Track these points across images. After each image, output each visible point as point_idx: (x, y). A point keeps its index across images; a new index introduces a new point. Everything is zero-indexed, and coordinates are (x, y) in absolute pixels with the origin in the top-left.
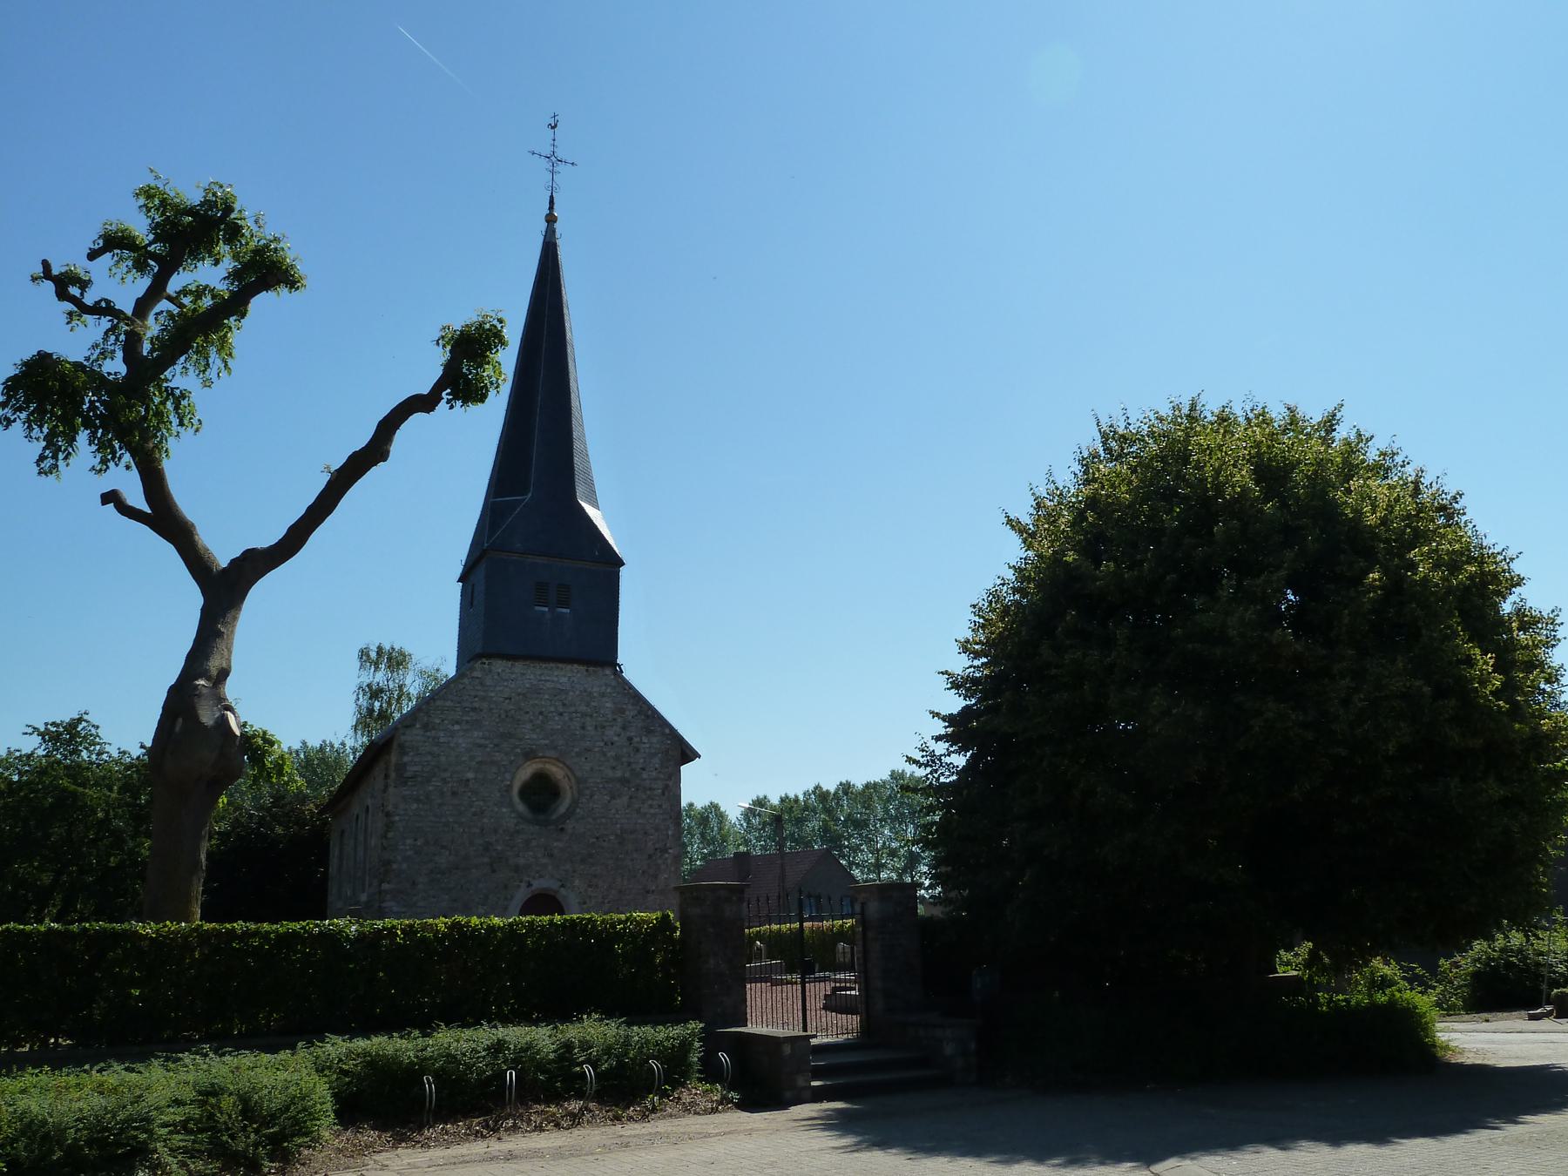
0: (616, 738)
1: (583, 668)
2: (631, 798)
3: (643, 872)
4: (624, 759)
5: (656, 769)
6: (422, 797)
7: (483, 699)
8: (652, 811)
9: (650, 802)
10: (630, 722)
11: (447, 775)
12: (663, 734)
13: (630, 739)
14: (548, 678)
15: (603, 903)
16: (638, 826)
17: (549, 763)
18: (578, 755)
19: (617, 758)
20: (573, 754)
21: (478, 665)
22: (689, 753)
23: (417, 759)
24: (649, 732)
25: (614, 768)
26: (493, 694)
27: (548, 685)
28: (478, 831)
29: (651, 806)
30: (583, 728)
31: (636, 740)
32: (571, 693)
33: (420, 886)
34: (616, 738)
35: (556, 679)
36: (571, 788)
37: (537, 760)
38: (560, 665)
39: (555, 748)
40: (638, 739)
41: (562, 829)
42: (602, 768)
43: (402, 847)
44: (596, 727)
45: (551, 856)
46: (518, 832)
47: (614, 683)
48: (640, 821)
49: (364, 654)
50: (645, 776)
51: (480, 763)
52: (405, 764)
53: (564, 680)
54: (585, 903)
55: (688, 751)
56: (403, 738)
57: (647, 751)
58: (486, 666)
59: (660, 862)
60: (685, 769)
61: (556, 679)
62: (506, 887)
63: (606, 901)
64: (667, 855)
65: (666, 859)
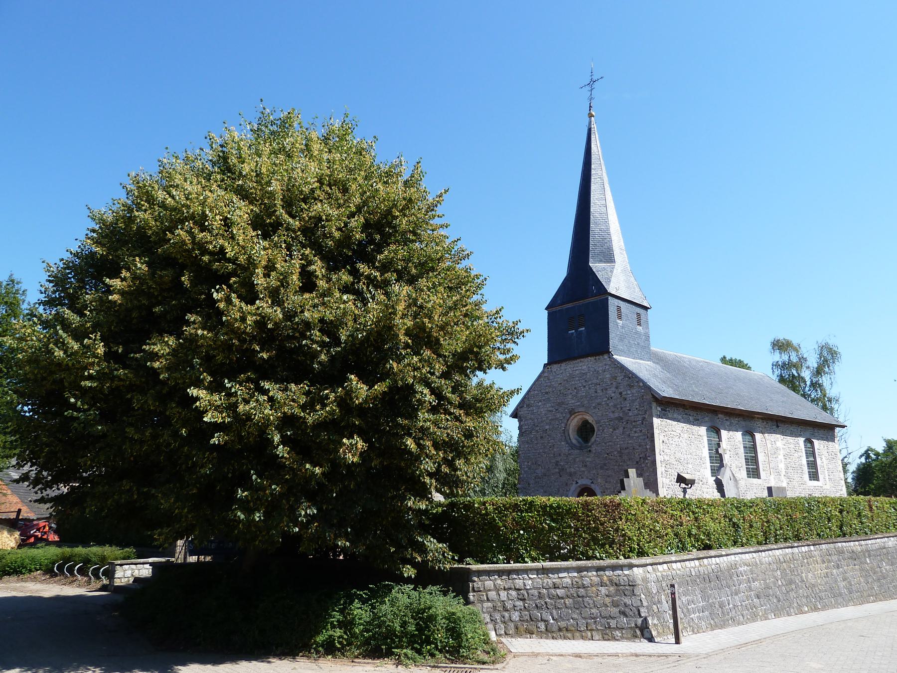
0: (613, 395)
1: (593, 358)
2: (624, 428)
4: (618, 406)
7: (550, 387)
8: (636, 435)
9: (634, 429)
11: (538, 428)
13: (621, 393)
18: (595, 408)
19: (615, 406)
20: (592, 408)
23: (526, 423)
24: (631, 387)
25: (613, 412)
27: (577, 372)
29: (635, 432)
32: (588, 374)
34: (613, 395)
38: (582, 360)
40: (625, 393)
41: (590, 451)
42: (607, 413)
44: (602, 391)
45: (586, 466)
46: (569, 454)
47: (609, 363)
48: (629, 442)
53: (584, 367)
56: (520, 413)
57: (631, 398)
58: (549, 369)
62: (567, 484)
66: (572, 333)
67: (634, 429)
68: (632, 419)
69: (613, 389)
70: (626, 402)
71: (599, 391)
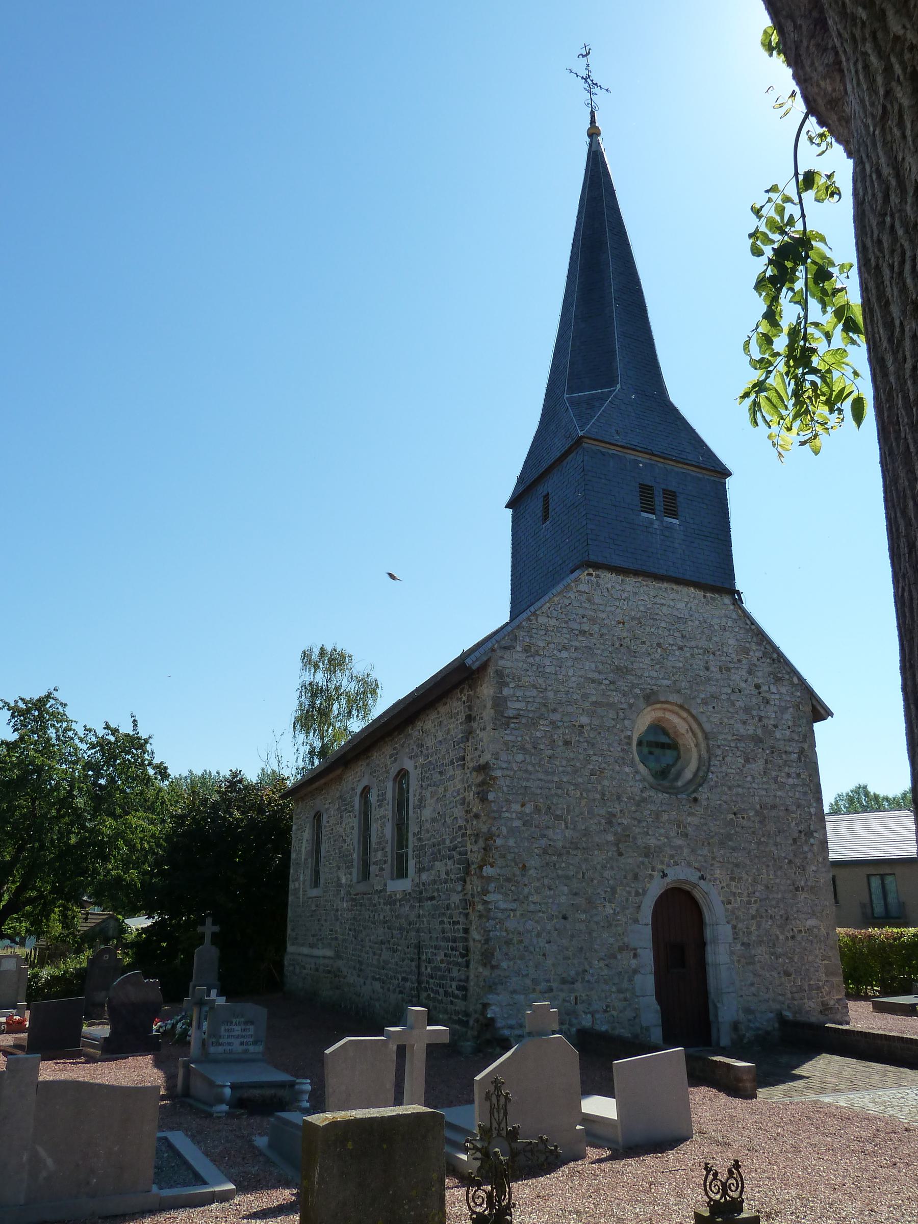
0: (743, 685)
1: (700, 594)
2: (766, 761)
3: (790, 862)
4: (754, 713)
5: (789, 728)
6: (527, 746)
7: (593, 620)
8: (791, 781)
9: (786, 769)
10: (755, 666)
11: (556, 717)
12: (792, 684)
13: (758, 687)
14: (663, 602)
15: (749, 903)
16: (778, 800)
17: (670, 711)
18: (705, 702)
20: (699, 701)
21: (584, 576)
22: (822, 712)
23: (519, 693)
24: (778, 680)
25: (744, 723)
26: (603, 615)
28: (598, 796)
29: (788, 775)
30: (707, 669)
31: (764, 688)
32: (690, 623)
33: (532, 872)
34: (743, 685)
35: (672, 603)
36: (697, 745)
37: (658, 706)
38: (675, 587)
39: (679, 692)
41: (695, 800)
42: (732, 722)
43: (507, 815)
47: (734, 616)
48: (779, 793)
49: (306, 656)
51: (594, 704)
52: (505, 699)
54: (729, 903)
55: (819, 708)
56: (501, 663)
57: (777, 702)
58: (593, 578)
59: (806, 849)
60: (818, 727)
61: (672, 603)
62: (636, 877)
63: (753, 900)
64: (812, 840)
65: (812, 845)
66: (651, 522)
68: (781, 745)
69: (744, 673)
70: (768, 706)
71: (712, 668)
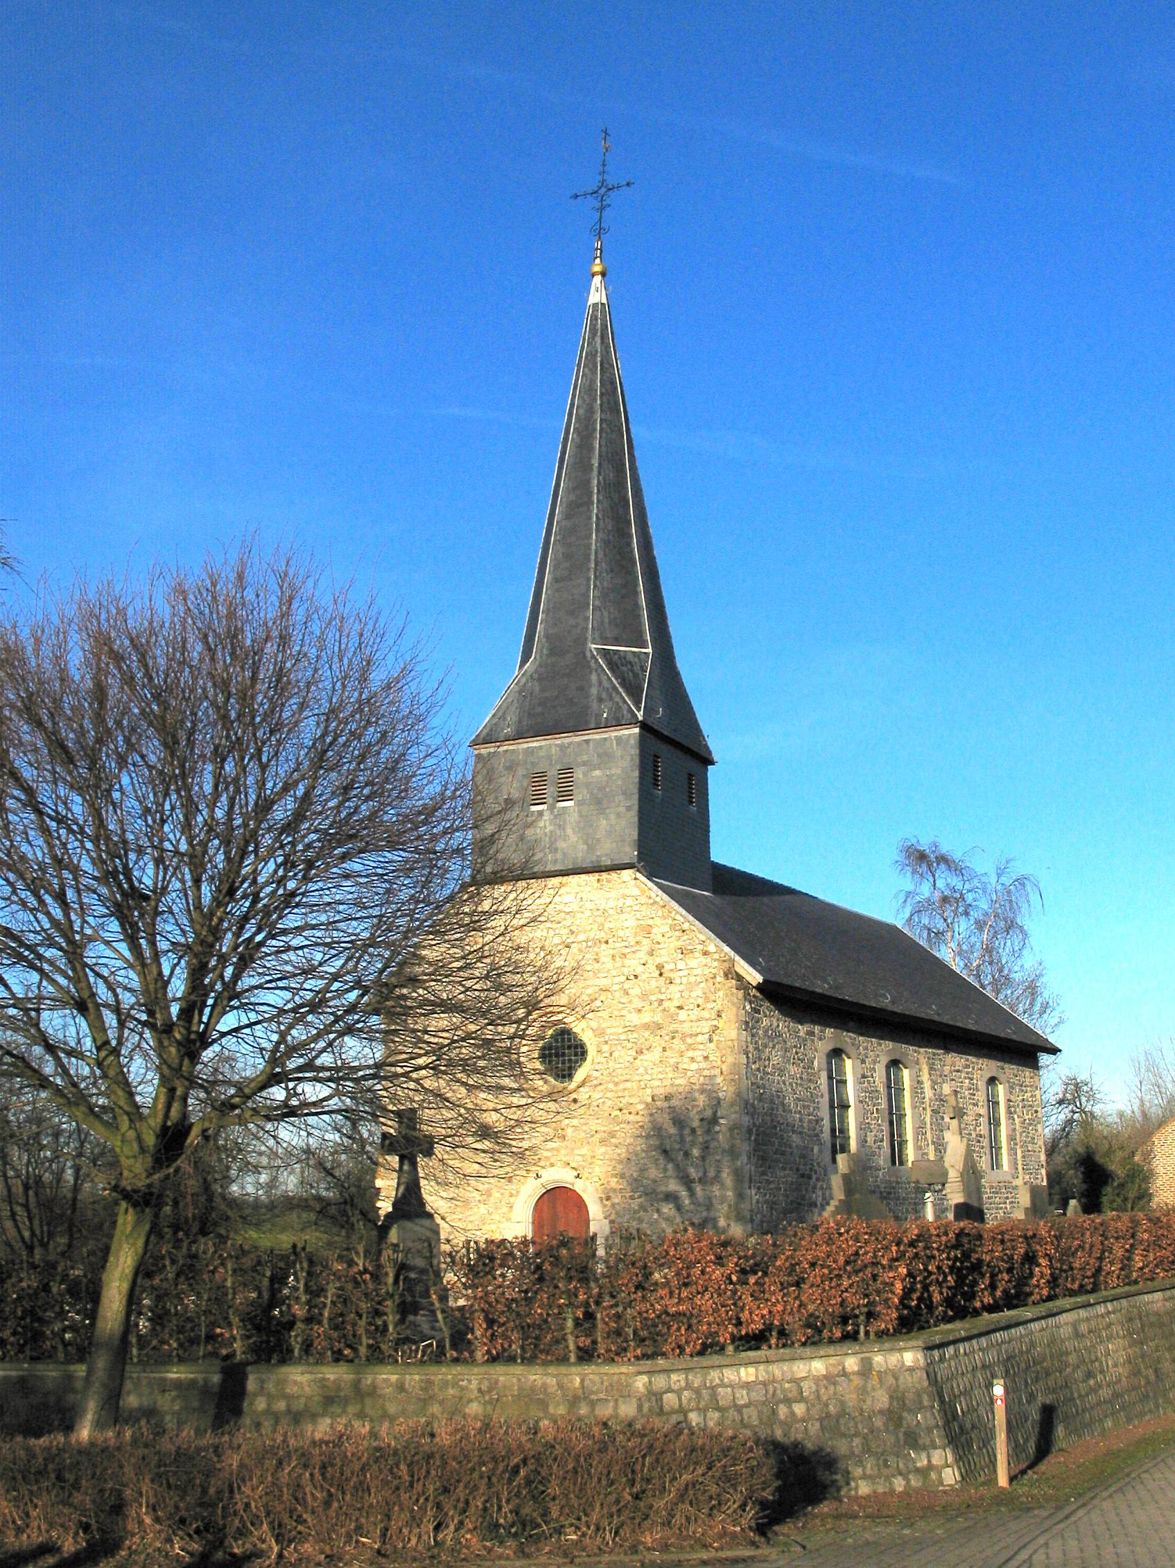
2: (664, 1050)
9: (690, 1054)
19: (644, 996)
40: (672, 966)
50: (682, 1015)
57: (684, 980)
67: (690, 1054)
68: (686, 1027)
70: (671, 986)
71: (603, 959)
